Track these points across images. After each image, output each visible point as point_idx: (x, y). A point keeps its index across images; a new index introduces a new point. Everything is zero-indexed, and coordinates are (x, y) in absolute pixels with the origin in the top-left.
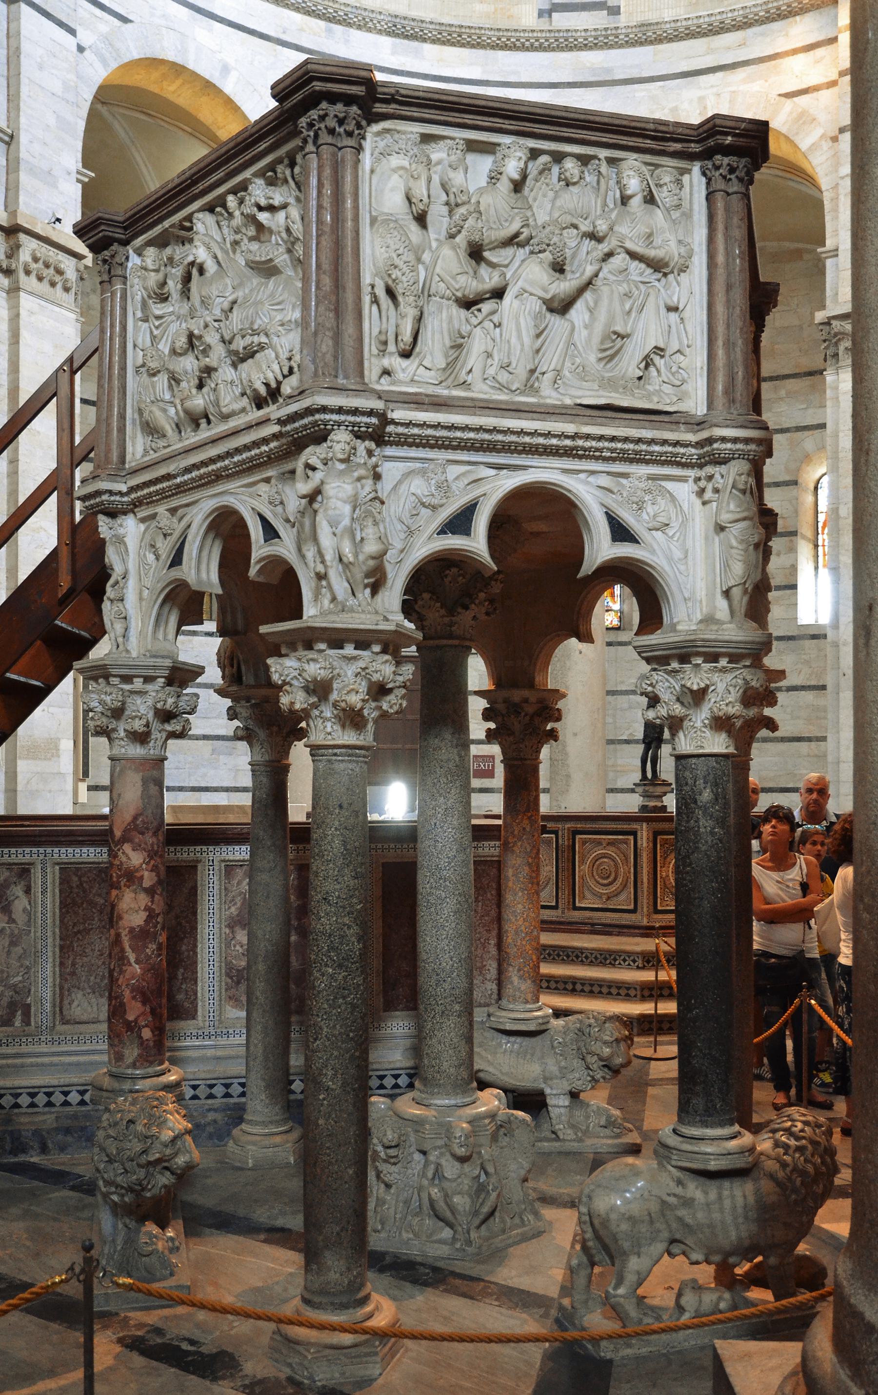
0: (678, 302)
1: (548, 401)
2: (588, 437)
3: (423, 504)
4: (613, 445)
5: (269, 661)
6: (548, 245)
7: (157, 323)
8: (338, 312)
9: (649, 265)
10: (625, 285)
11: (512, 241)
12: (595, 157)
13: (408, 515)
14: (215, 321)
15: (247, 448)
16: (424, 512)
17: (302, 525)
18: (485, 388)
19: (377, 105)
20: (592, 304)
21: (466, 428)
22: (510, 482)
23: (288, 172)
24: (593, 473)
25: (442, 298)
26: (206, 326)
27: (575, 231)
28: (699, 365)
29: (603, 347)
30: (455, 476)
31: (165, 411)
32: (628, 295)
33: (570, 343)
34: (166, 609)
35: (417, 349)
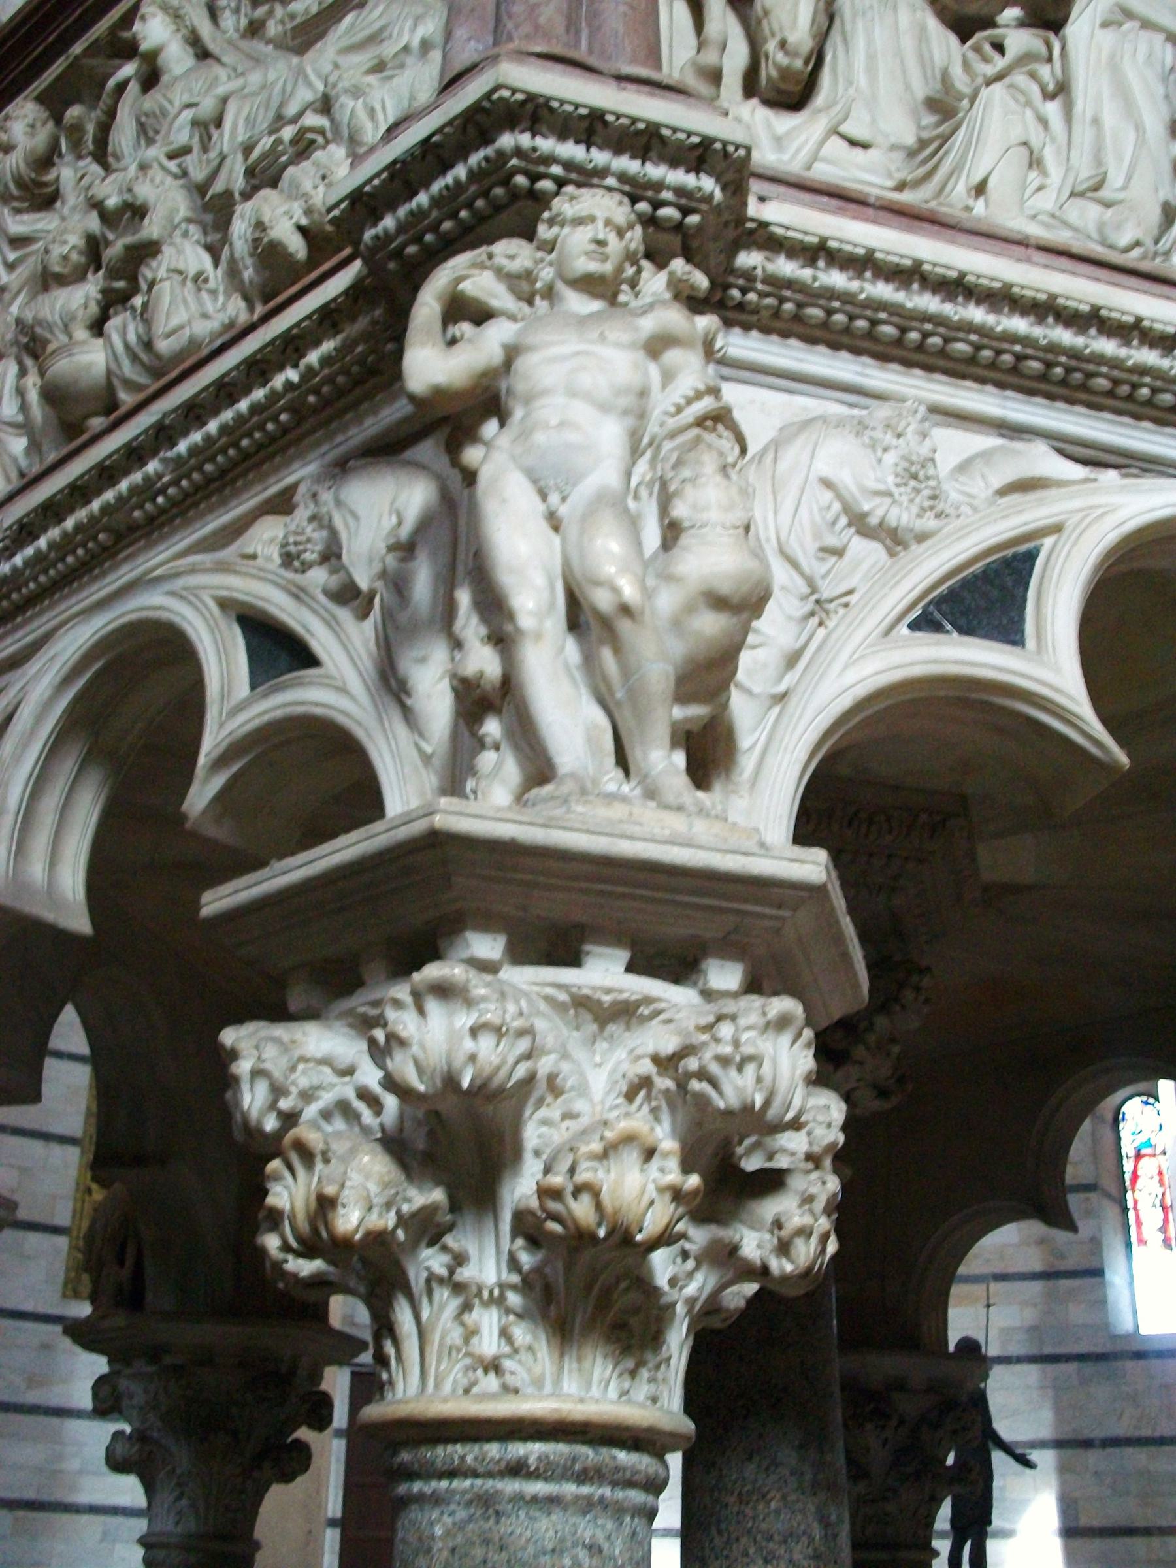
3: (860, 523)
5: (229, 1036)
7: (12, 256)
13: (812, 546)
14: (171, 157)
17: (399, 585)
30: (954, 461)
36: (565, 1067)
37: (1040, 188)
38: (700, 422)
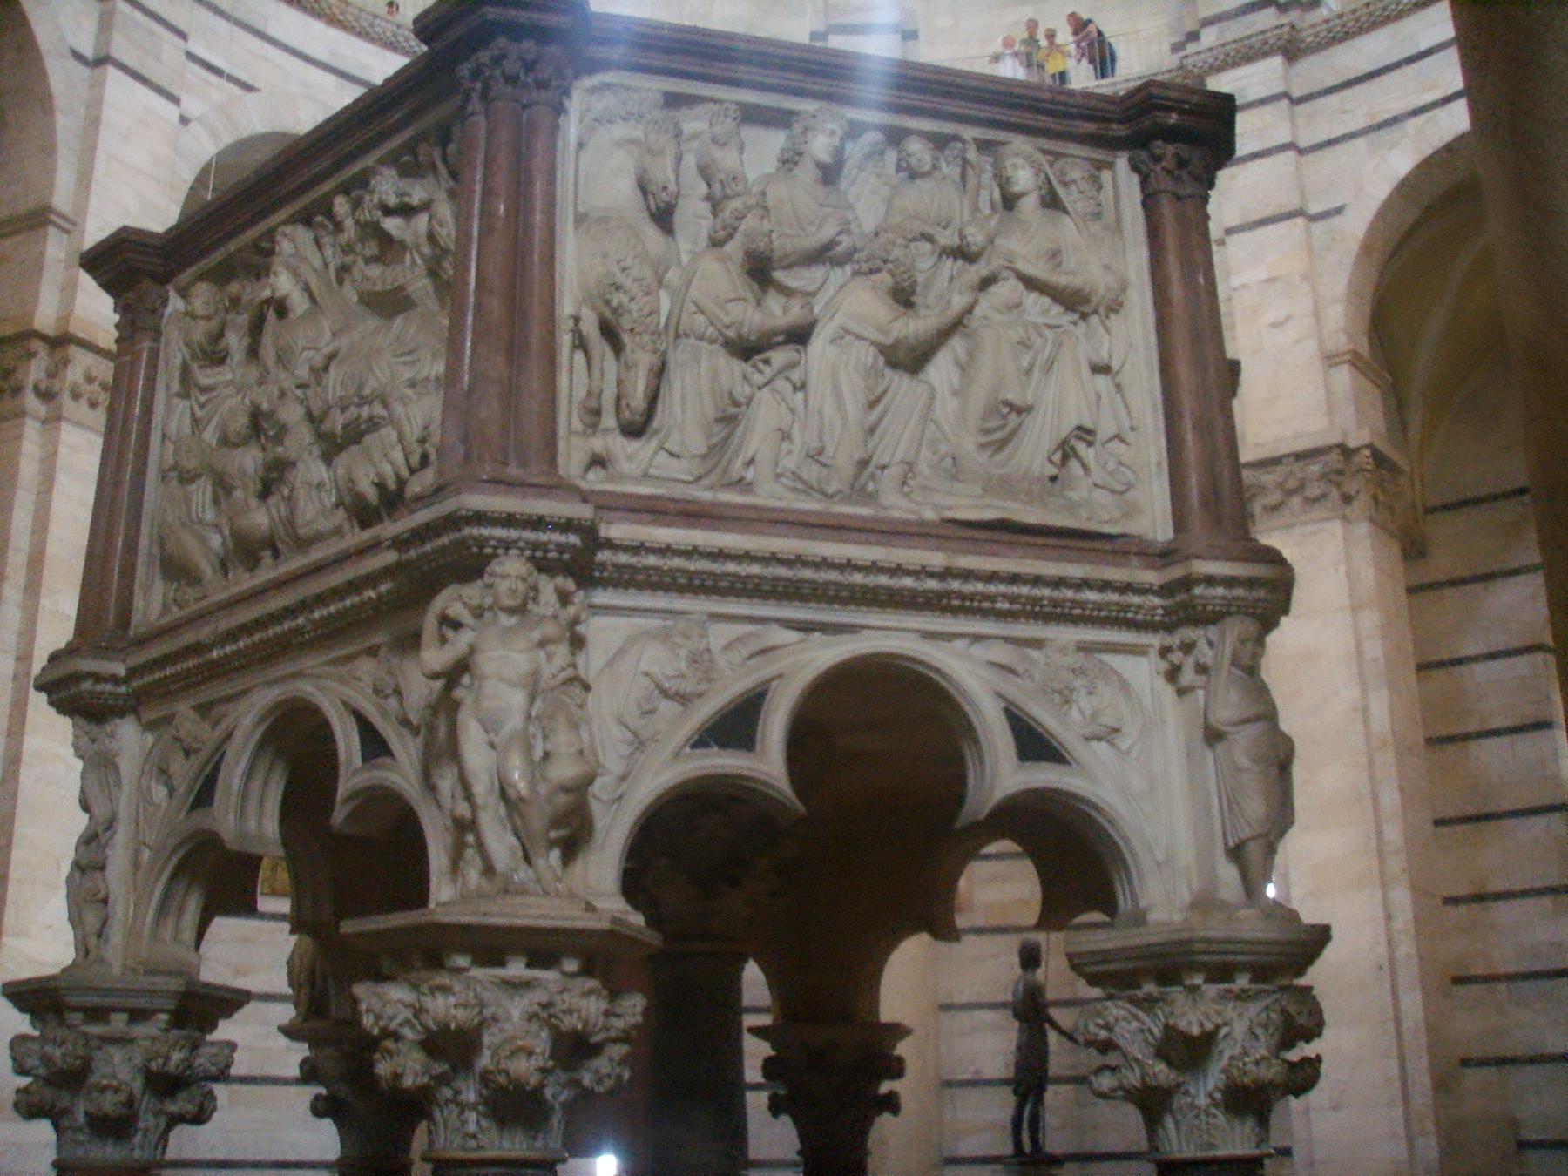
1: (896, 514)
2: (967, 575)
3: (664, 693)
4: (1014, 589)
6: (885, 261)
7: (203, 399)
8: (515, 351)
10: (1020, 329)
11: (822, 255)
12: (957, 138)
14: (299, 387)
15: (338, 593)
16: (667, 708)
17: (432, 730)
18: (778, 489)
20: (963, 356)
21: (747, 557)
22: (826, 654)
23: (436, 154)
24: (978, 638)
25: (701, 338)
26: (283, 394)
27: (928, 246)
28: (1154, 459)
30: (723, 642)
31: (203, 541)
32: (1025, 344)
34: (180, 890)
35: (655, 424)
36: (500, 1011)
37: (790, 452)
38: (564, 683)
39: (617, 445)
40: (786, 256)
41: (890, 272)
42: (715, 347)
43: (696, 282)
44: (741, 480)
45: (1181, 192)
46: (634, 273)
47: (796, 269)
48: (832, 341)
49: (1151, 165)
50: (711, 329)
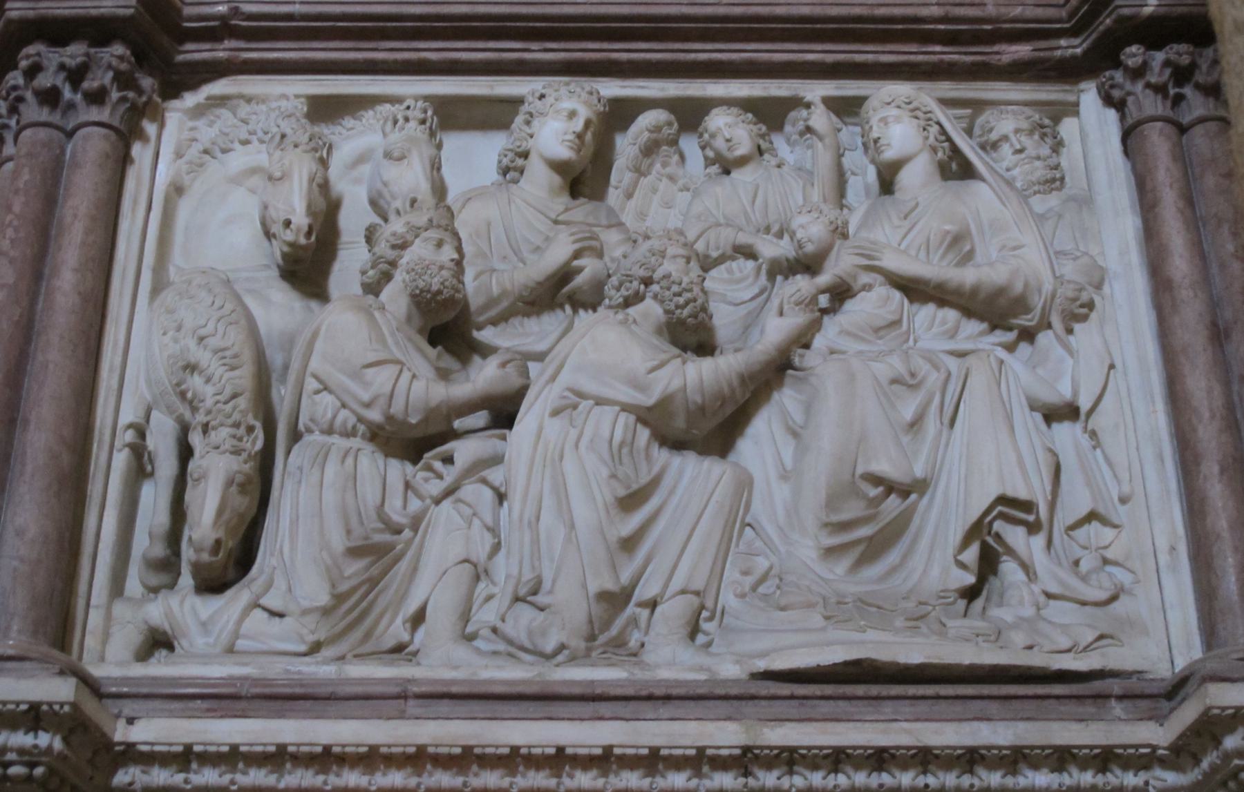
0: (1075, 393)
6: (647, 282)
9: (968, 313)
11: (556, 293)
12: (796, 103)
19: (189, 46)
20: (798, 417)
25: (329, 431)
27: (750, 264)
28: (1162, 544)
29: (835, 518)
32: (907, 382)
33: (737, 519)
37: (489, 598)
39: (184, 608)
40: (491, 303)
41: (655, 297)
42: (356, 442)
43: (319, 345)
44: (399, 649)
45: (1186, 120)
46: (213, 342)
47: (516, 321)
48: (556, 413)
49: (1128, 86)
50: (344, 413)
